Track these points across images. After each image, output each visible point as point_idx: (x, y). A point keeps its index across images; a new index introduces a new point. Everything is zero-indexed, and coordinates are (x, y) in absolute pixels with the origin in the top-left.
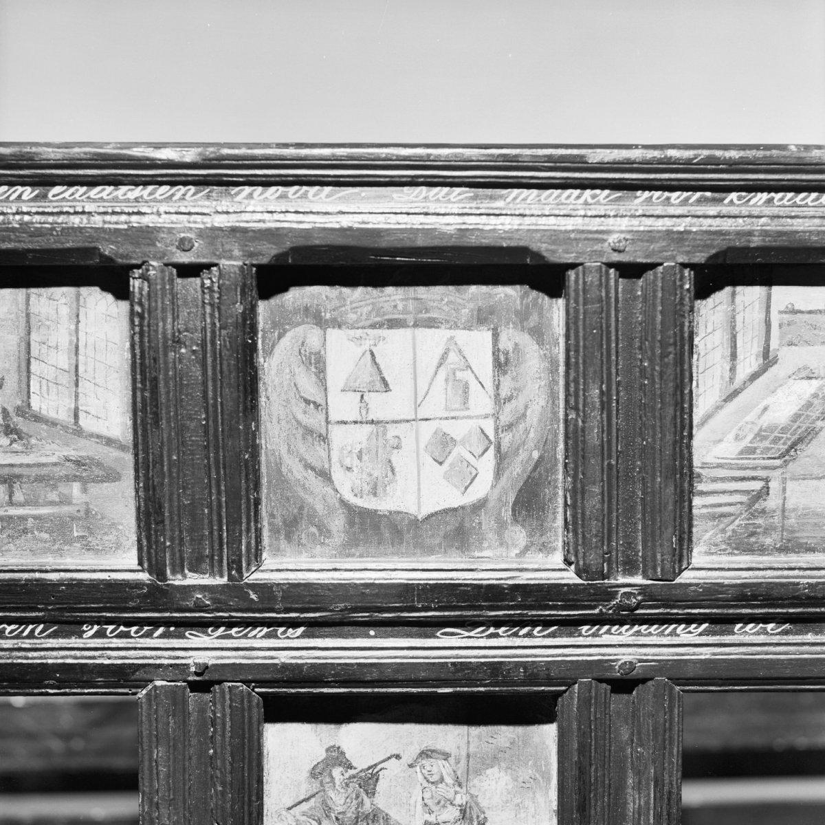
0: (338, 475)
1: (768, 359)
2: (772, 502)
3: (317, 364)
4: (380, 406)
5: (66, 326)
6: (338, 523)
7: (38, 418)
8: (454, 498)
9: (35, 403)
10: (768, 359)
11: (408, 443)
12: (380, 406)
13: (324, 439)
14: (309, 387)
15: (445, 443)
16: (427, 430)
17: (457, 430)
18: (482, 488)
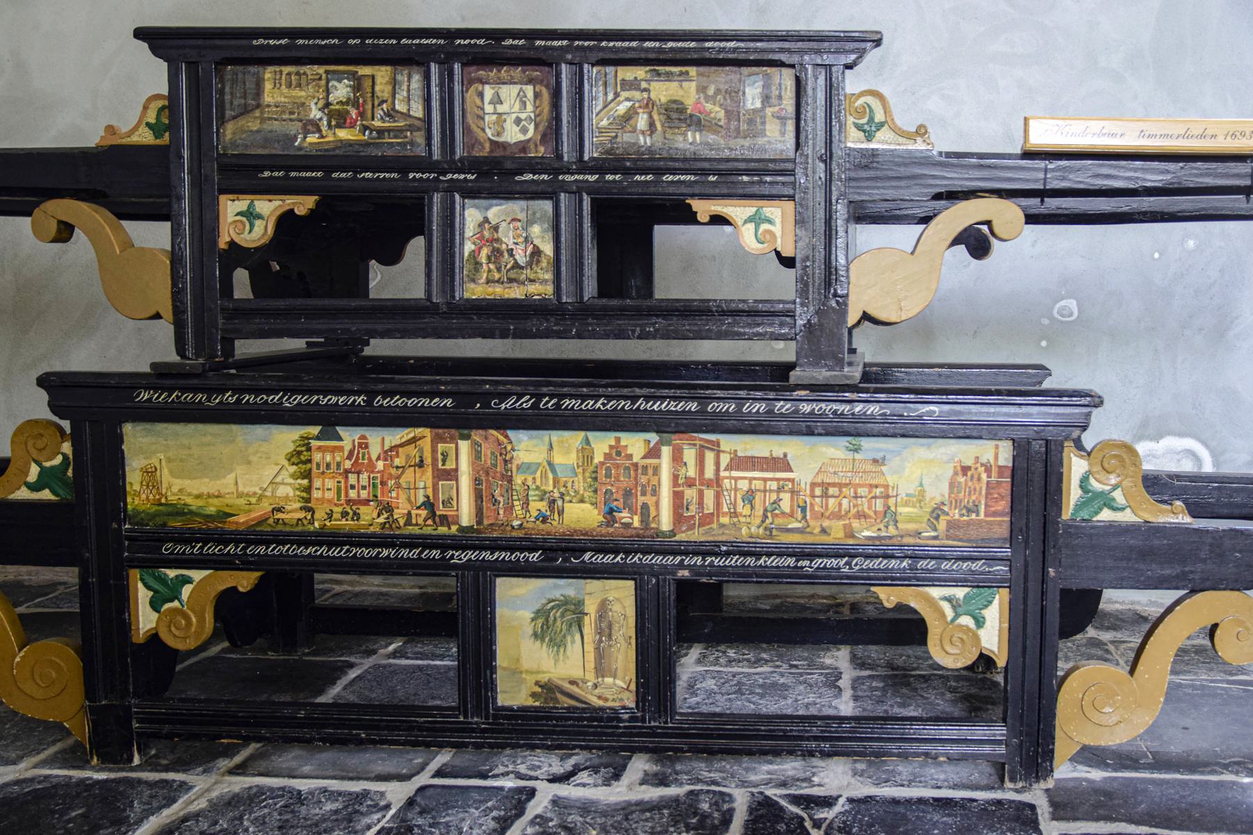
0: (487, 130)
1: (617, 95)
2: (619, 140)
3: (481, 95)
4: (500, 109)
5: (406, 84)
6: (487, 145)
7: (398, 112)
8: (522, 138)
9: (397, 107)
10: (617, 95)
11: (508, 121)
12: (500, 109)
13: (483, 119)
14: (478, 102)
15: (518, 121)
16: (514, 116)
17: (523, 116)
18: (530, 134)
